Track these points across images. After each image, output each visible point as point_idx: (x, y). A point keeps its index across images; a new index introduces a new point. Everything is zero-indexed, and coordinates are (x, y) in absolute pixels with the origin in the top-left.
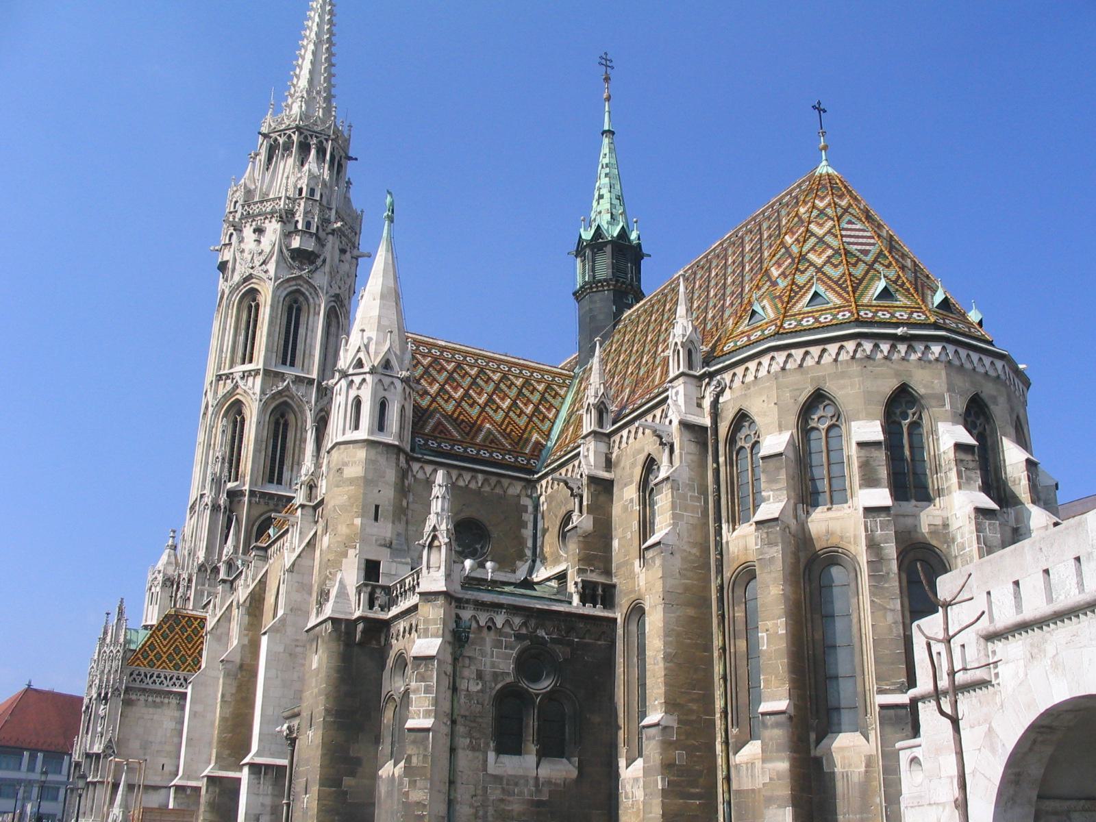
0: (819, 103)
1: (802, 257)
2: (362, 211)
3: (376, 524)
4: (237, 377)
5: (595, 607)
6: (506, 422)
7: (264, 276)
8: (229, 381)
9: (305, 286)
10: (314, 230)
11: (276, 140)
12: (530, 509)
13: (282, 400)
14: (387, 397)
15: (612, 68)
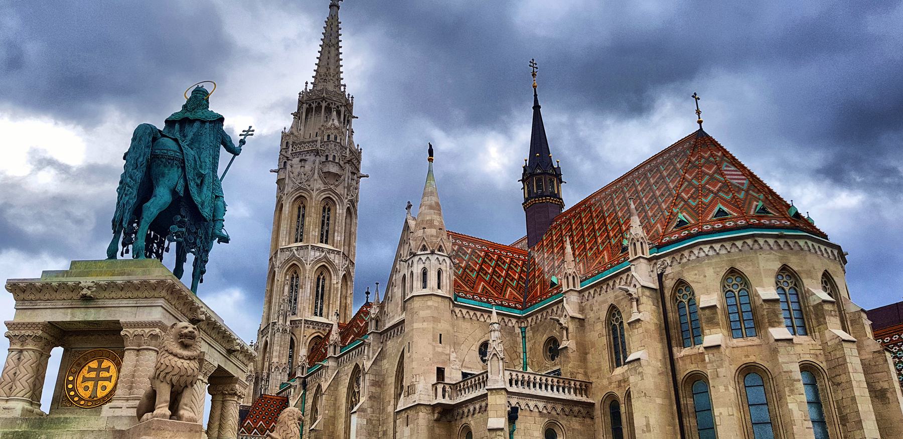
0: (695, 94)
2: (361, 149)
5: (582, 396)
6: (492, 281)
7: (308, 188)
9: (333, 195)
10: (337, 161)
11: (310, 105)
13: (322, 264)
15: (537, 68)
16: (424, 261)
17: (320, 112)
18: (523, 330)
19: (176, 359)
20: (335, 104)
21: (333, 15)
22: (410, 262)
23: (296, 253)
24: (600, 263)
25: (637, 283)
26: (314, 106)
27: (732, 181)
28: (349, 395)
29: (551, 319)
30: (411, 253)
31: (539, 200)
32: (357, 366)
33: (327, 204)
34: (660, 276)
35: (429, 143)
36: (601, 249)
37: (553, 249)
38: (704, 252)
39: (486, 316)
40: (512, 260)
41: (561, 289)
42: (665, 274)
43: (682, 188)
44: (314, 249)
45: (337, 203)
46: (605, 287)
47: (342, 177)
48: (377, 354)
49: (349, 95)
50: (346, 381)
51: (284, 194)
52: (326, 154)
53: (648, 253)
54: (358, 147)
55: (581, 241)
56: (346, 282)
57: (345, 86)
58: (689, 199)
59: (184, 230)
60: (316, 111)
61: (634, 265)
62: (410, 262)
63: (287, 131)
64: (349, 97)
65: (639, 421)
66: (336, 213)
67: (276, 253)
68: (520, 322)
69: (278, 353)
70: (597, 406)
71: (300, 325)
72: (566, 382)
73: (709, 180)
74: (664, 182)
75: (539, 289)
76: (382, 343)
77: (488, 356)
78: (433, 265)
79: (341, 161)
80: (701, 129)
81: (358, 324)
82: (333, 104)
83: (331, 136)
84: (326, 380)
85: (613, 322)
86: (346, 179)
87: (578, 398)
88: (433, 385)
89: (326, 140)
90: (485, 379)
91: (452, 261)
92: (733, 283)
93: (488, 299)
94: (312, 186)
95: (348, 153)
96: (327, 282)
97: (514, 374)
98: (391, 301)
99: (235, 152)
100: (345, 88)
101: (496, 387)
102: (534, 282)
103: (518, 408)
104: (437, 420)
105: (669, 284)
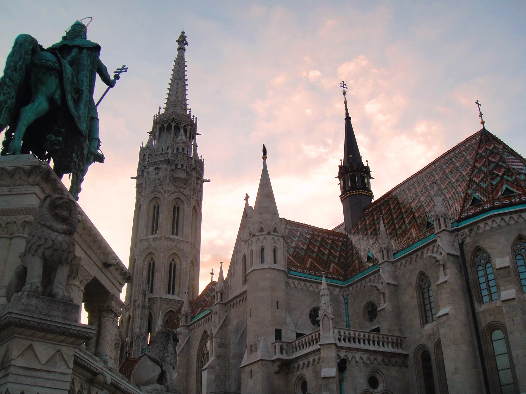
1: (491, 173)
2: (204, 160)
3: (278, 310)
4: (151, 240)
5: (398, 349)
6: (318, 258)
7: (162, 191)
8: (145, 243)
9: (182, 196)
10: (185, 168)
11: (163, 125)
12: (343, 302)
13: (173, 252)
15: (346, 88)
16: (262, 241)
17: (171, 130)
18: (345, 297)
19: (49, 231)
20: (182, 124)
21: (180, 56)
23: (152, 243)
24: (409, 239)
25: (442, 252)
26: (165, 125)
27: (513, 167)
28: (199, 356)
29: (371, 286)
30: (250, 234)
31: (353, 193)
32: (205, 332)
33: (177, 204)
34: (461, 245)
35: (264, 145)
36: (408, 227)
37: (367, 231)
38: (496, 223)
39: (314, 285)
40: (333, 241)
41: (376, 262)
42: (465, 243)
43: (474, 174)
44: (167, 240)
45: (185, 203)
46: (414, 258)
47: (189, 182)
48: (222, 321)
49: (193, 117)
50: (196, 344)
51: (142, 196)
52: (175, 163)
53: (451, 227)
54: (201, 158)
55: (391, 223)
56: (193, 266)
57: (190, 109)
58: (480, 182)
59: (61, 139)
60: (167, 130)
61: (439, 237)
63: (144, 146)
64: (193, 118)
65: (449, 366)
66: (184, 211)
67: (136, 243)
68: (342, 291)
69: (139, 325)
70: (411, 356)
72: (385, 337)
73: (495, 166)
74: (458, 171)
75: (357, 265)
76: (226, 311)
77: (320, 317)
78: (268, 243)
79: (187, 168)
80: (484, 128)
81: (205, 298)
82: (181, 124)
83: (179, 149)
85: (422, 286)
86: (192, 183)
87: (395, 350)
88: (272, 344)
89: (175, 152)
90: (317, 336)
91: (285, 241)
92: (521, 248)
93: (315, 272)
94: (165, 189)
95: (193, 162)
97: (342, 331)
98: (234, 276)
99: (110, 84)
100: (190, 111)
101: (328, 342)
102: (353, 258)
103: (346, 360)
104: (277, 373)
105: (469, 251)
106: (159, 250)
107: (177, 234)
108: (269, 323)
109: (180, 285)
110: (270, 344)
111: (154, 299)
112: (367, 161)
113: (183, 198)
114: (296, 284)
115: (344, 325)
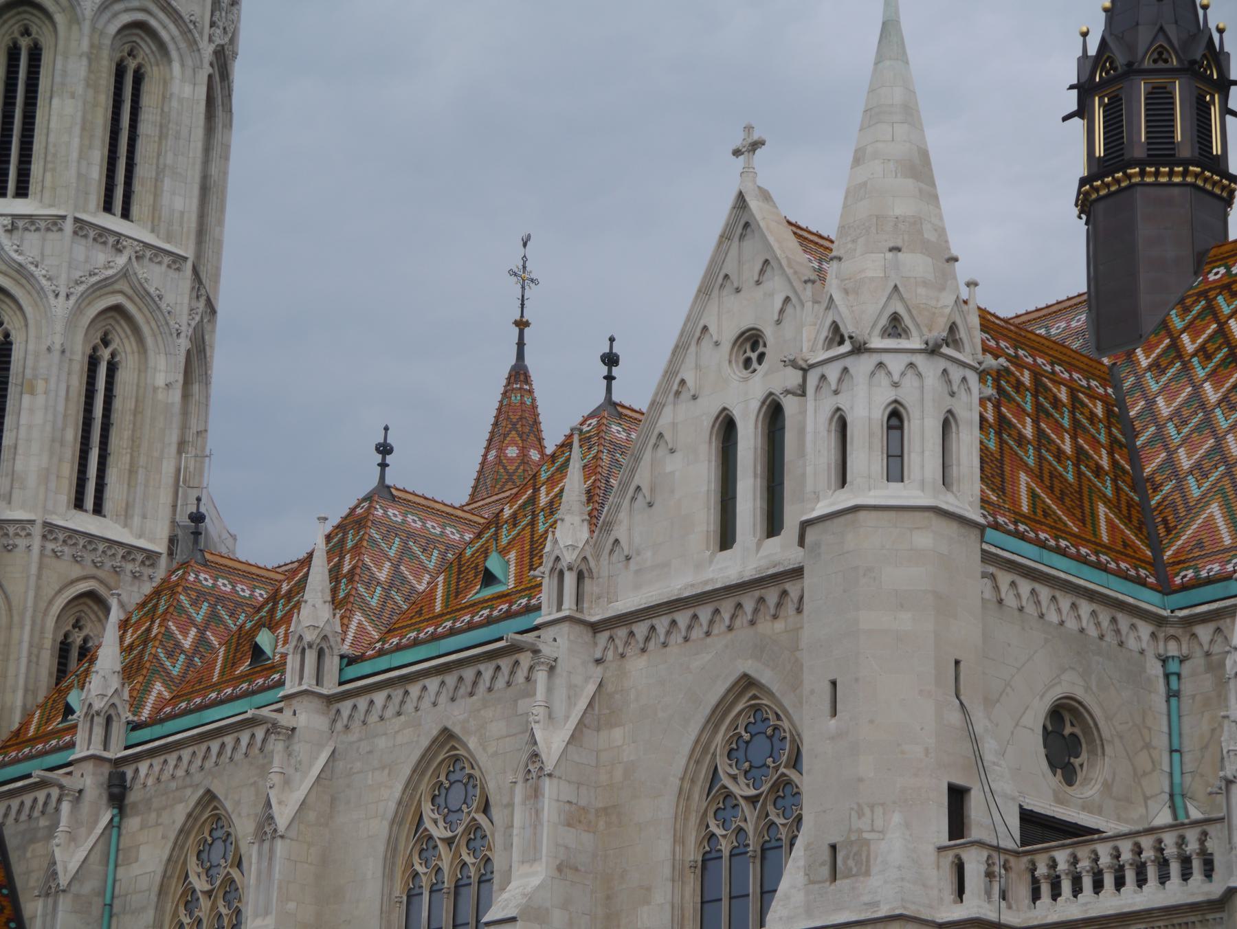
9: (162, 15)
14: (954, 411)
18: (1173, 667)
22: (833, 372)
28: (395, 849)
30: (837, 335)
33: (131, 53)
45: (174, 54)
48: (582, 704)
62: (833, 372)
71: (21, 542)
76: (598, 661)
84: (287, 782)
96: (125, 377)
106: (44, 282)
107: (126, 214)
108: (927, 751)
109: (132, 471)
110: (931, 849)
111: (11, 530)
112: (1221, 31)
113: (167, 30)
114: (1004, 587)
115: (1163, 792)
